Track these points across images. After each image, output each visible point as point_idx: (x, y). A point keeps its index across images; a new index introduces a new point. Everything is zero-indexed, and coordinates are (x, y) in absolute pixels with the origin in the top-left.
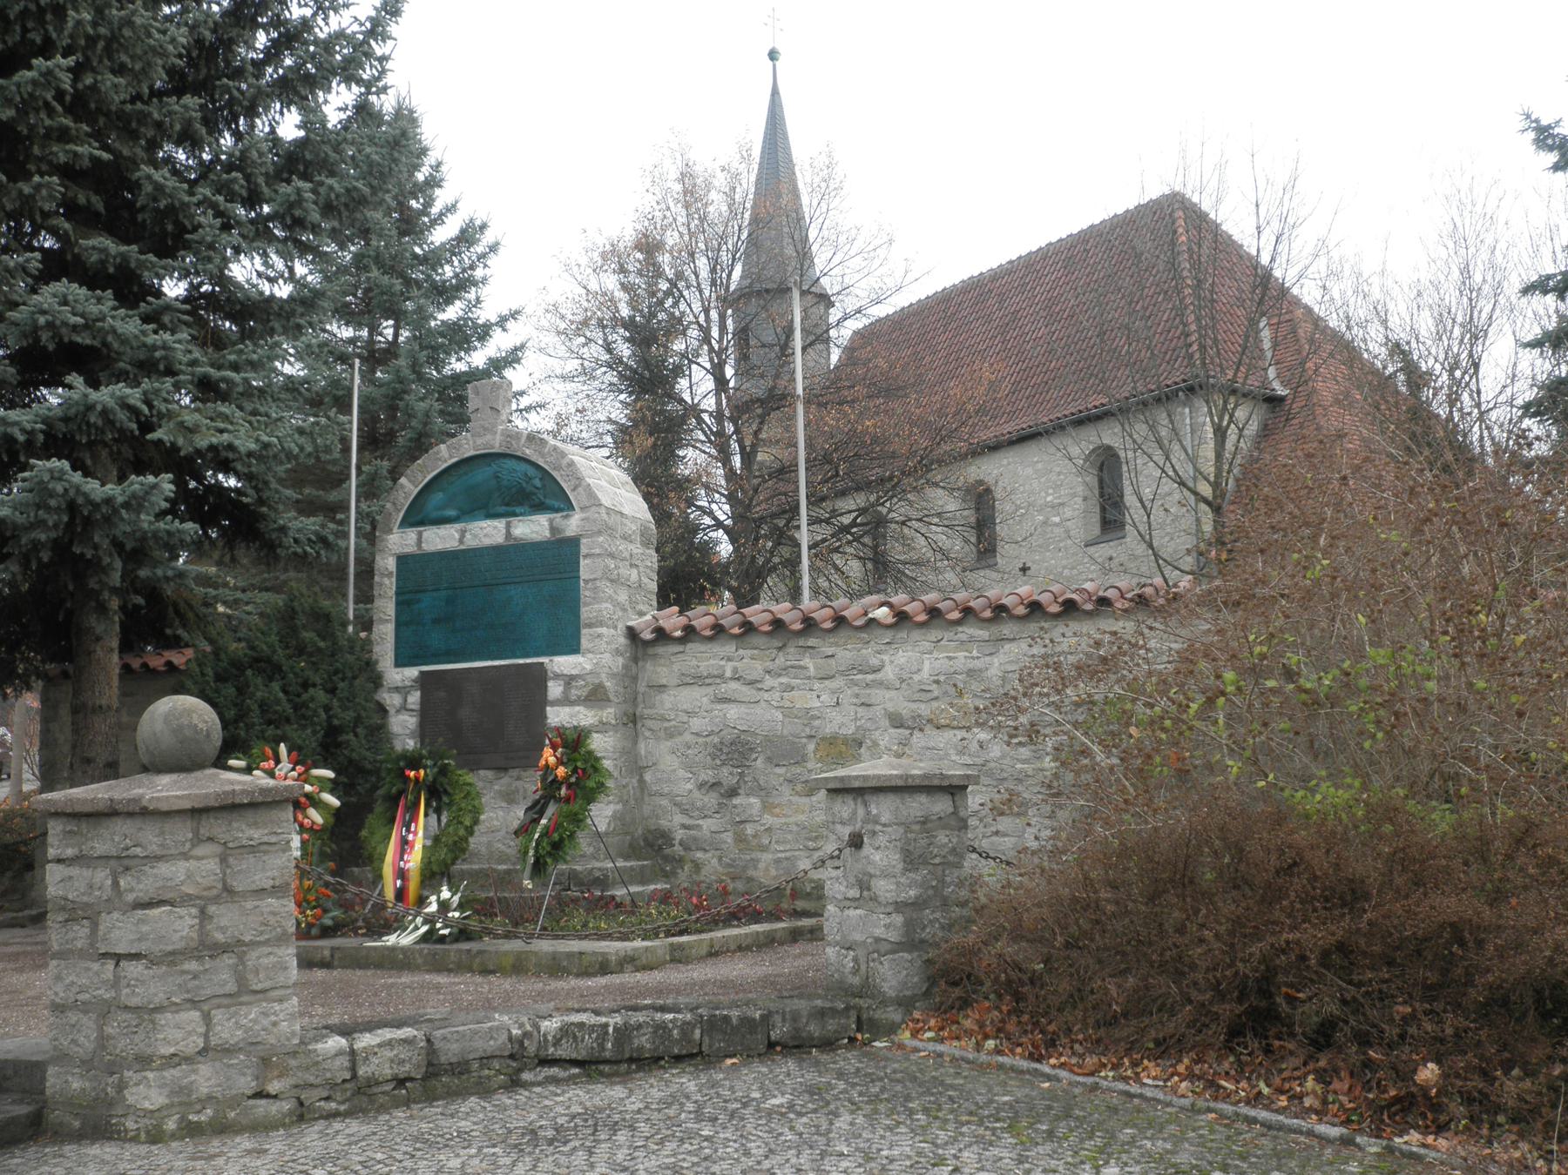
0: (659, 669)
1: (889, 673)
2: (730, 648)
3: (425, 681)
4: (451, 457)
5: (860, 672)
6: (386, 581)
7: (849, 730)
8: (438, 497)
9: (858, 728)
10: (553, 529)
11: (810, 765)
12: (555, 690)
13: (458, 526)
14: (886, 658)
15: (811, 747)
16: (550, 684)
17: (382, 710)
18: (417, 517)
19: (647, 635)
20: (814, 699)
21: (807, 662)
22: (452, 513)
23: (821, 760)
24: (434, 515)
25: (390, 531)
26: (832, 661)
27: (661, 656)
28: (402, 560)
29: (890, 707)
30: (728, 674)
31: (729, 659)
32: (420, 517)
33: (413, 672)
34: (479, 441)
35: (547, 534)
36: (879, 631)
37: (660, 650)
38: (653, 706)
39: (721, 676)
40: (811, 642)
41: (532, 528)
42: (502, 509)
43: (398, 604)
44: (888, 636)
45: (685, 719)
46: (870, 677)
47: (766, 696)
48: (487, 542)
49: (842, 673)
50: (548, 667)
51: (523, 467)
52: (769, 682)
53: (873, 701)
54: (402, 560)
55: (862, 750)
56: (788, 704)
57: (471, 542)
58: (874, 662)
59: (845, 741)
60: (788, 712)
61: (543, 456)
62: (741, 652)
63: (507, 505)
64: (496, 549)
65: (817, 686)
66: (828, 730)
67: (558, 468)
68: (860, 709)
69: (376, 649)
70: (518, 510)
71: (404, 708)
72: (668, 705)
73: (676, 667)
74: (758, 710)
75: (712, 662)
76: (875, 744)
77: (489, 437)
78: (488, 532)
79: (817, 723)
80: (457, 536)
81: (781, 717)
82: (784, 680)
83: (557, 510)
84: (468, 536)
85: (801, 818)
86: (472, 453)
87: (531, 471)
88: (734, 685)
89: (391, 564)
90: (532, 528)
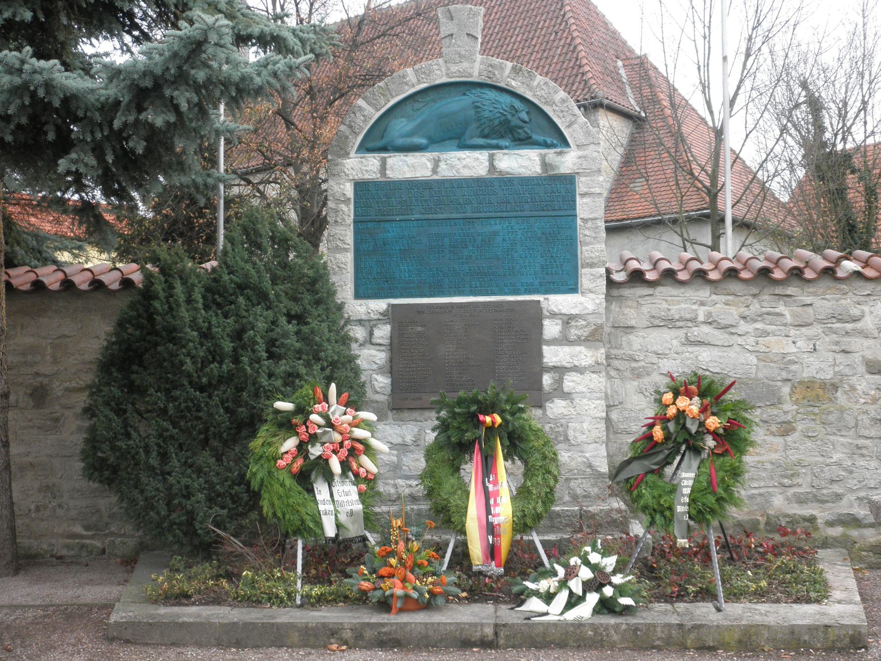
0: (626, 311)
1: (868, 323)
2: (704, 293)
3: (394, 315)
4: (419, 82)
5: (840, 321)
6: (343, 207)
7: (828, 375)
8: (400, 127)
9: (835, 373)
10: (545, 165)
11: (788, 406)
12: (551, 328)
13: (428, 155)
14: (866, 308)
15: (786, 390)
16: (546, 323)
17: (346, 340)
18: (378, 141)
19: (619, 277)
20: (791, 344)
21: (781, 308)
22: (424, 141)
23: (796, 402)
24: (400, 142)
25: (346, 155)
26: (810, 310)
27: (627, 298)
28: (361, 187)
29: (869, 355)
30: (701, 318)
31: (702, 304)
32: (380, 144)
33: (380, 305)
34: (454, 68)
35: (538, 169)
36: (860, 283)
37: (626, 292)
38: (619, 347)
39: (694, 320)
40: (790, 291)
41: (521, 162)
42: (481, 141)
43: (357, 232)
44: (868, 288)
45: (655, 360)
46: (849, 326)
47: (740, 340)
48: (466, 173)
49: (820, 321)
50: (544, 305)
51: (506, 99)
52: (743, 327)
53: (853, 349)
54: (361, 187)
55: (839, 394)
56: (763, 349)
57: (445, 172)
58: (855, 311)
59: (823, 385)
60: (763, 357)
61: (531, 89)
62: (714, 297)
63: (486, 136)
64: (477, 182)
65: (793, 332)
66: (806, 375)
67: (551, 103)
68: (838, 356)
69: (333, 279)
70: (502, 142)
71: (369, 340)
72: (636, 346)
73: (645, 309)
74: (732, 354)
75: (683, 305)
76: (853, 388)
77: (465, 65)
78: (468, 163)
79: (793, 367)
80: (430, 166)
81: (755, 361)
82: (759, 325)
83: (547, 145)
84: (442, 166)
85: (774, 456)
86: (445, 80)
87: (517, 104)
88: (706, 329)
89: (349, 190)
90: (521, 162)
